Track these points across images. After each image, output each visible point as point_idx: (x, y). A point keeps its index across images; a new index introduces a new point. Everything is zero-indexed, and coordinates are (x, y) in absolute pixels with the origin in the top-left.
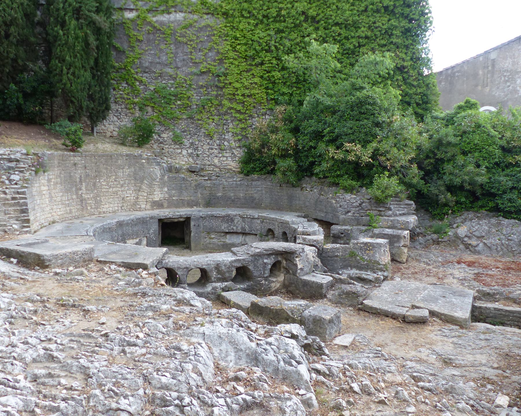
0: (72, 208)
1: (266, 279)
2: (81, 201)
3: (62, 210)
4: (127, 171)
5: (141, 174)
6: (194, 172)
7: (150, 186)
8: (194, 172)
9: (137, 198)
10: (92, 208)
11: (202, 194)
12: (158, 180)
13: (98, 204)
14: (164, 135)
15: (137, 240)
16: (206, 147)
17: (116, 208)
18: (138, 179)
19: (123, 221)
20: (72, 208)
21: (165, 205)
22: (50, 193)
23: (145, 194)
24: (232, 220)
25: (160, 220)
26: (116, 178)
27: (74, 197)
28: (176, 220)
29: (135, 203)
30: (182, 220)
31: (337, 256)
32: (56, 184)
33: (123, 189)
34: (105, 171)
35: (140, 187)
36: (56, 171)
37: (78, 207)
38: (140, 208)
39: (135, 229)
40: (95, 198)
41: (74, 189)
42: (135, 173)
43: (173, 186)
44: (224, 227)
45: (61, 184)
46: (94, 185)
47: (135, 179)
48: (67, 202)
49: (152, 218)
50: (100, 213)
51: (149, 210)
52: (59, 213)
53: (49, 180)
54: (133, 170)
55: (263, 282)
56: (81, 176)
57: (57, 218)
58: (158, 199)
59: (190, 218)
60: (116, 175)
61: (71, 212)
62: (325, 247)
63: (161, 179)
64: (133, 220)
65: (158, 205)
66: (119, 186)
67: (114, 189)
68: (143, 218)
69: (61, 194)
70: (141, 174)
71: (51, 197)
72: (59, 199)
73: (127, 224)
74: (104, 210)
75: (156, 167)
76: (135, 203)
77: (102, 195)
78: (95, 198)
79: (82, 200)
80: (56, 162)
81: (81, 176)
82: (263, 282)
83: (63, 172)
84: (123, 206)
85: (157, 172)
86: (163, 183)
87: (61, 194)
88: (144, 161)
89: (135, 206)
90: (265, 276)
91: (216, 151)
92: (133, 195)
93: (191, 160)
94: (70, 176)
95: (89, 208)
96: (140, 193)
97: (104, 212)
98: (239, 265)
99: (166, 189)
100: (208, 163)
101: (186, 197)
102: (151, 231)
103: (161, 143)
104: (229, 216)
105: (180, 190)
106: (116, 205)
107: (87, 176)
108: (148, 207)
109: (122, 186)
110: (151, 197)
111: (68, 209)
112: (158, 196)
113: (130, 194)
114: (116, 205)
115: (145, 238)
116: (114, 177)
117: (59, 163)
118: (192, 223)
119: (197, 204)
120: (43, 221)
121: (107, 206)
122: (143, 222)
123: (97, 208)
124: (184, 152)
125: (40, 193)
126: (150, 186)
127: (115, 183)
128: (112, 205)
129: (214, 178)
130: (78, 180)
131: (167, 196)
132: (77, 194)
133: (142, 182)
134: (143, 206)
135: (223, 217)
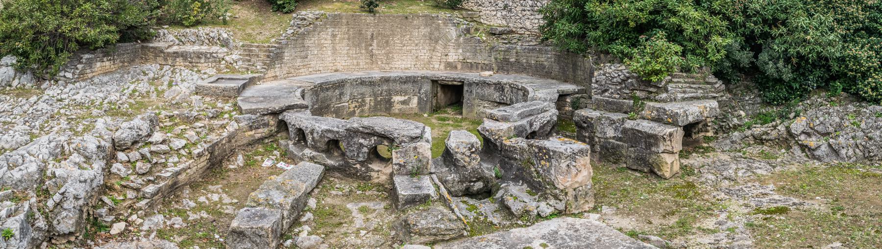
1: (362, 163)
2: (372, 56)
4: (424, 31)
5: (436, 34)
6: (495, 34)
7: (445, 46)
8: (495, 34)
11: (496, 59)
15: (406, 98)
16: (519, 8)
18: (433, 39)
19: (390, 77)
21: (459, 66)
24: (503, 90)
25: (434, 82)
27: (363, 51)
28: (450, 83)
29: (429, 62)
30: (455, 83)
31: (516, 159)
35: (435, 47)
36: (344, 29)
37: (368, 61)
39: (404, 87)
40: (387, 54)
41: (363, 45)
44: (496, 96)
45: (349, 39)
46: (387, 42)
49: (423, 78)
50: (391, 68)
53: (334, 36)
55: (358, 166)
57: (339, 67)
61: (358, 64)
62: (507, 143)
63: (456, 40)
65: (450, 66)
68: (415, 77)
70: (436, 34)
71: (334, 50)
72: (345, 52)
73: (395, 81)
76: (429, 62)
78: (387, 54)
82: (358, 166)
85: (453, 32)
86: (458, 45)
90: (360, 159)
91: (528, 13)
93: (504, 22)
98: (330, 136)
99: (460, 51)
100: (520, 26)
101: (481, 59)
102: (422, 91)
104: (499, 83)
105: (475, 53)
108: (442, 67)
111: (355, 61)
112: (453, 57)
113: (424, 53)
115: (416, 98)
118: (466, 88)
119: (491, 69)
120: (321, 69)
122: (414, 82)
124: (499, 14)
125: (320, 46)
126: (445, 46)
129: (515, 41)
130: (369, 37)
132: (366, 49)
133: (437, 42)
134: (437, 66)
135: (495, 84)
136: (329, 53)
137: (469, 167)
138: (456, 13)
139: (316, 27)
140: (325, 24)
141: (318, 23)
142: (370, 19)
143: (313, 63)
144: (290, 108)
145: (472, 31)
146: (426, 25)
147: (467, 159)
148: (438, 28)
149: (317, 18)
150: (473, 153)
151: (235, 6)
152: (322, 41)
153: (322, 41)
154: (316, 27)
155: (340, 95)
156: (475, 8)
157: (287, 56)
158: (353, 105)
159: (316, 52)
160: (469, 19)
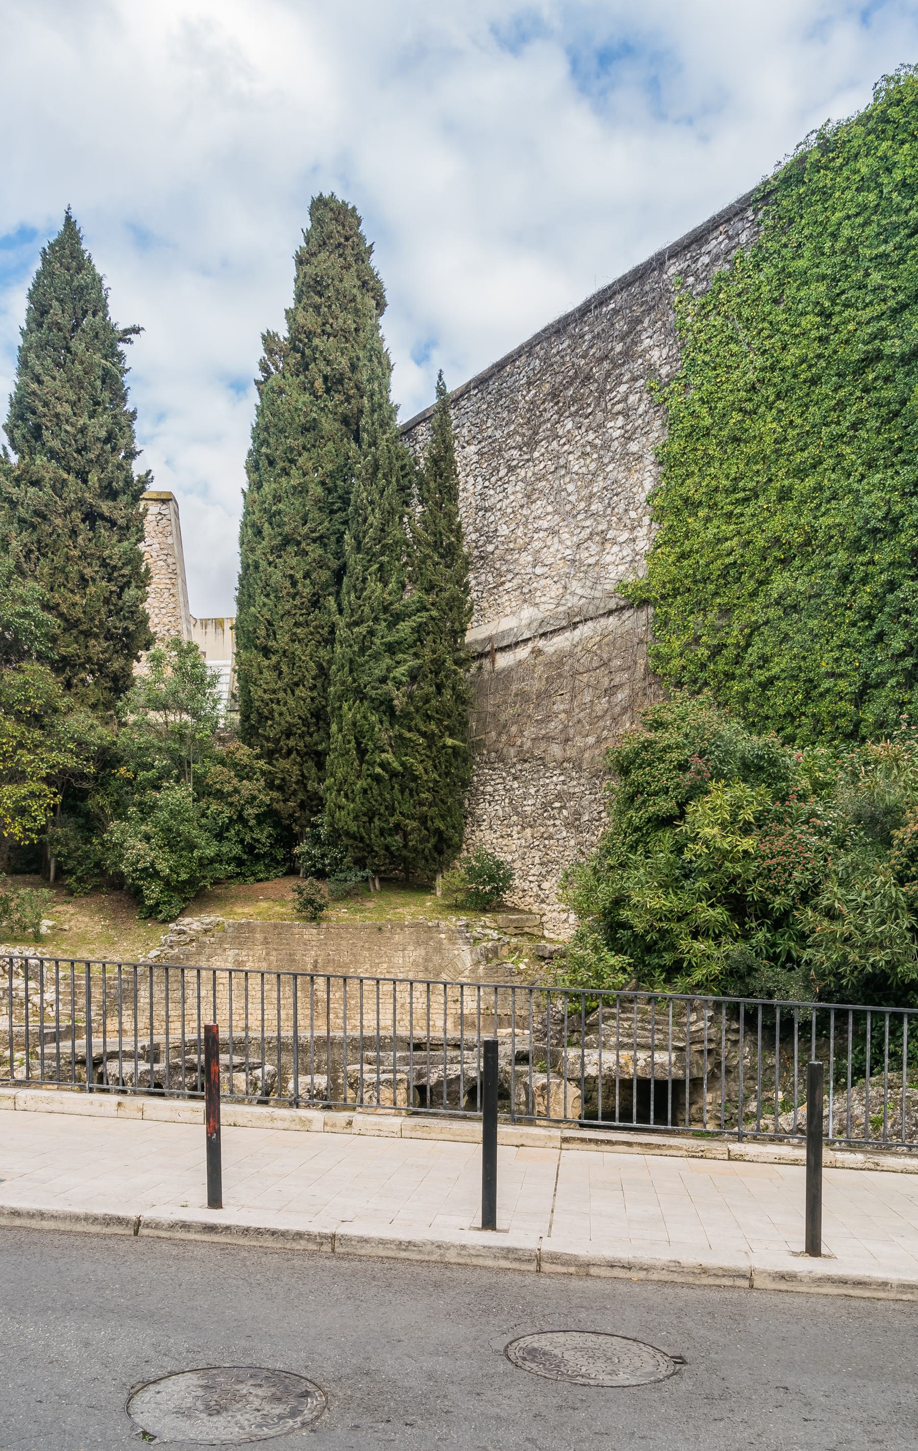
6: (543, 958)
8: (543, 958)
12: (467, 973)
14: (546, 885)
26: (388, 967)
34: (366, 953)
42: (427, 960)
47: (427, 969)
54: (423, 953)
56: (316, 962)
63: (473, 971)
70: (436, 959)
75: (465, 948)
80: (259, 936)
81: (316, 962)
83: (274, 953)
88: (443, 936)
94: (294, 960)
103: (543, 901)
116: (385, 966)
117: (266, 938)
138: (486, 919)
139: (202, 946)
140: (221, 942)
141: (206, 939)
142: (310, 933)
145: (504, 951)
146: (418, 944)
148: (439, 949)
149: (206, 931)
151: (60, 908)
154: (202, 946)
156: (535, 908)
160: (511, 930)
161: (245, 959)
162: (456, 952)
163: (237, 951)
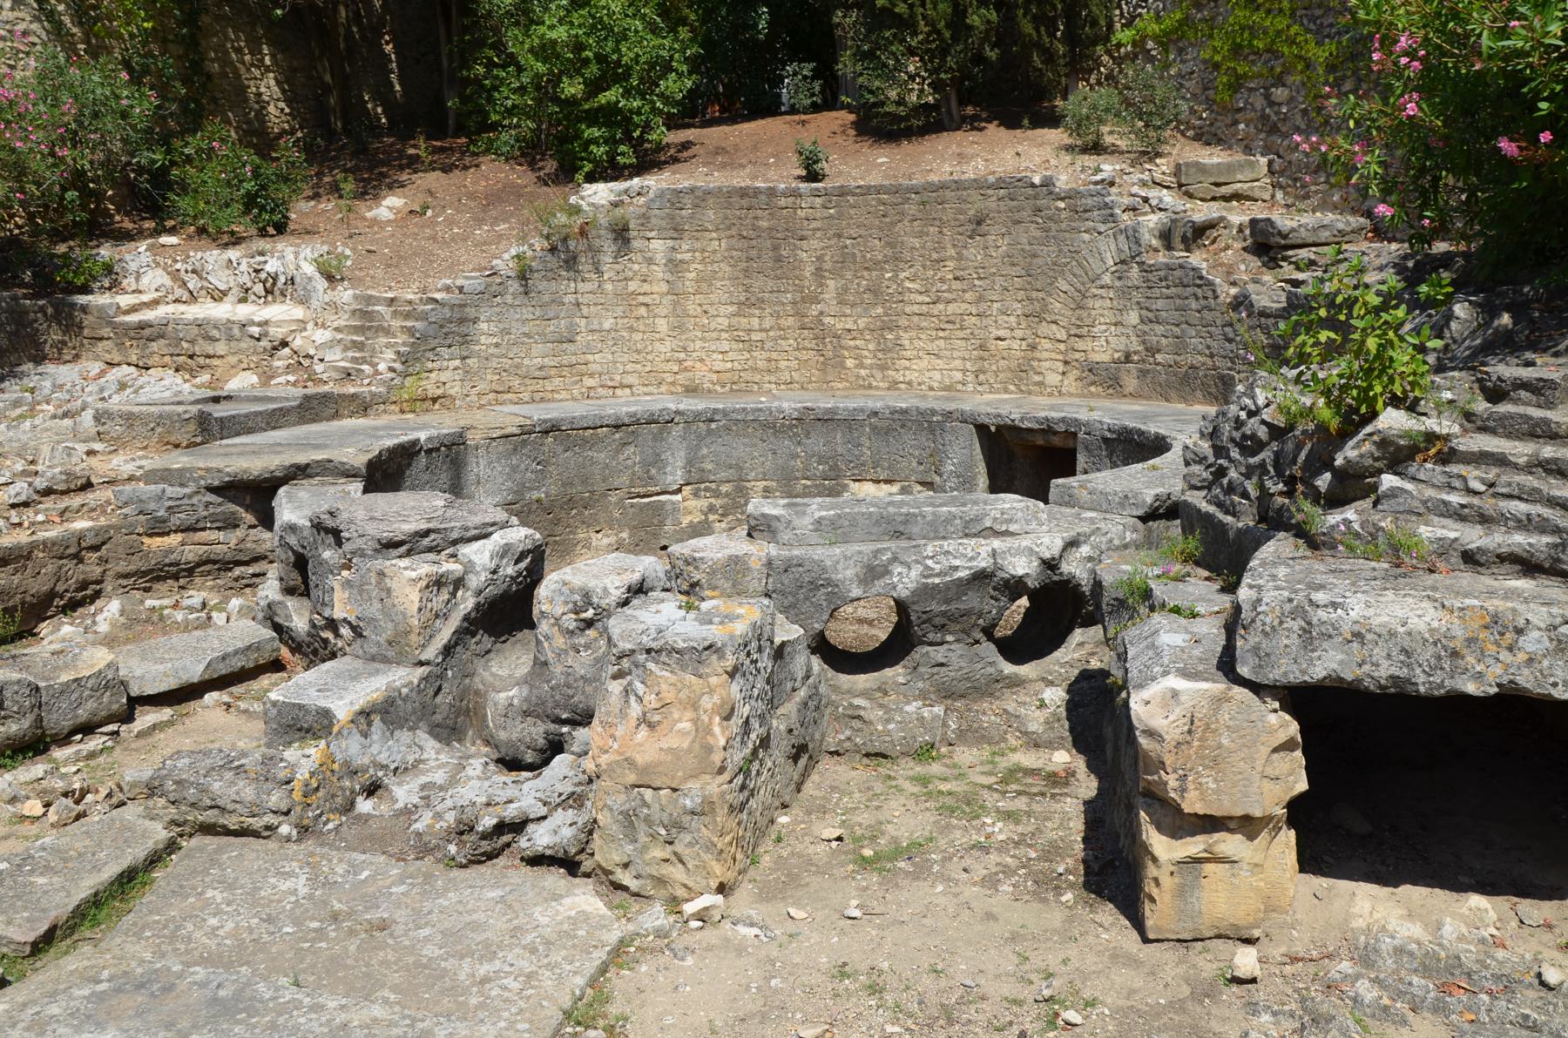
0: (774, 355)
3: (731, 355)
9: (1033, 347)
10: (861, 366)
13: (888, 354)
17: (958, 376)
19: (833, 411)
20: (774, 355)
22: (675, 304)
23: (1062, 335)
28: (1040, 442)
30: (1056, 441)
32: (705, 280)
33: (983, 306)
36: (717, 244)
38: (1040, 384)
43: (1160, 304)
48: (756, 337)
50: (894, 385)
51: (1071, 395)
52: (719, 366)
53: (674, 266)
57: (702, 375)
58: (1105, 358)
59: (1075, 434)
60: (960, 257)
64: (876, 414)
66: (968, 296)
67: (951, 308)
69: (732, 309)
70: (1049, 253)
74: (910, 376)
77: (903, 322)
79: (822, 334)
84: (981, 371)
87: (732, 309)
89: (1022, 373)
92: (1019, 333)
95: (850, 363)
96: (1044, 329)
97: (909, 383)
99: (1133, 317)
106: (958, 363)
107: (845, 259)
109: (981, 299)
110: (1080, 345)
113: (1006, 328)
114: (958, 363)
120: (630, 379)
121: (924, 364)
123: (883, 368)
127: (956, 285)
128: (940, 363)
130: (809, 270)
131: (1135, 345)
134: (1053, 379)
136: (662, 325)
137: (558, 669)
143: (597, 361)
144: (299, 472)
147: (560, 641)
150: (589, 624)
152: (633, 286)
153: (633, 286)
155: (647, 465)
157: (486, 331)
158: (703, 503)
159: (607, 325)
161: (687, 256)
162: (1086, 237)
163: (670, 243)
